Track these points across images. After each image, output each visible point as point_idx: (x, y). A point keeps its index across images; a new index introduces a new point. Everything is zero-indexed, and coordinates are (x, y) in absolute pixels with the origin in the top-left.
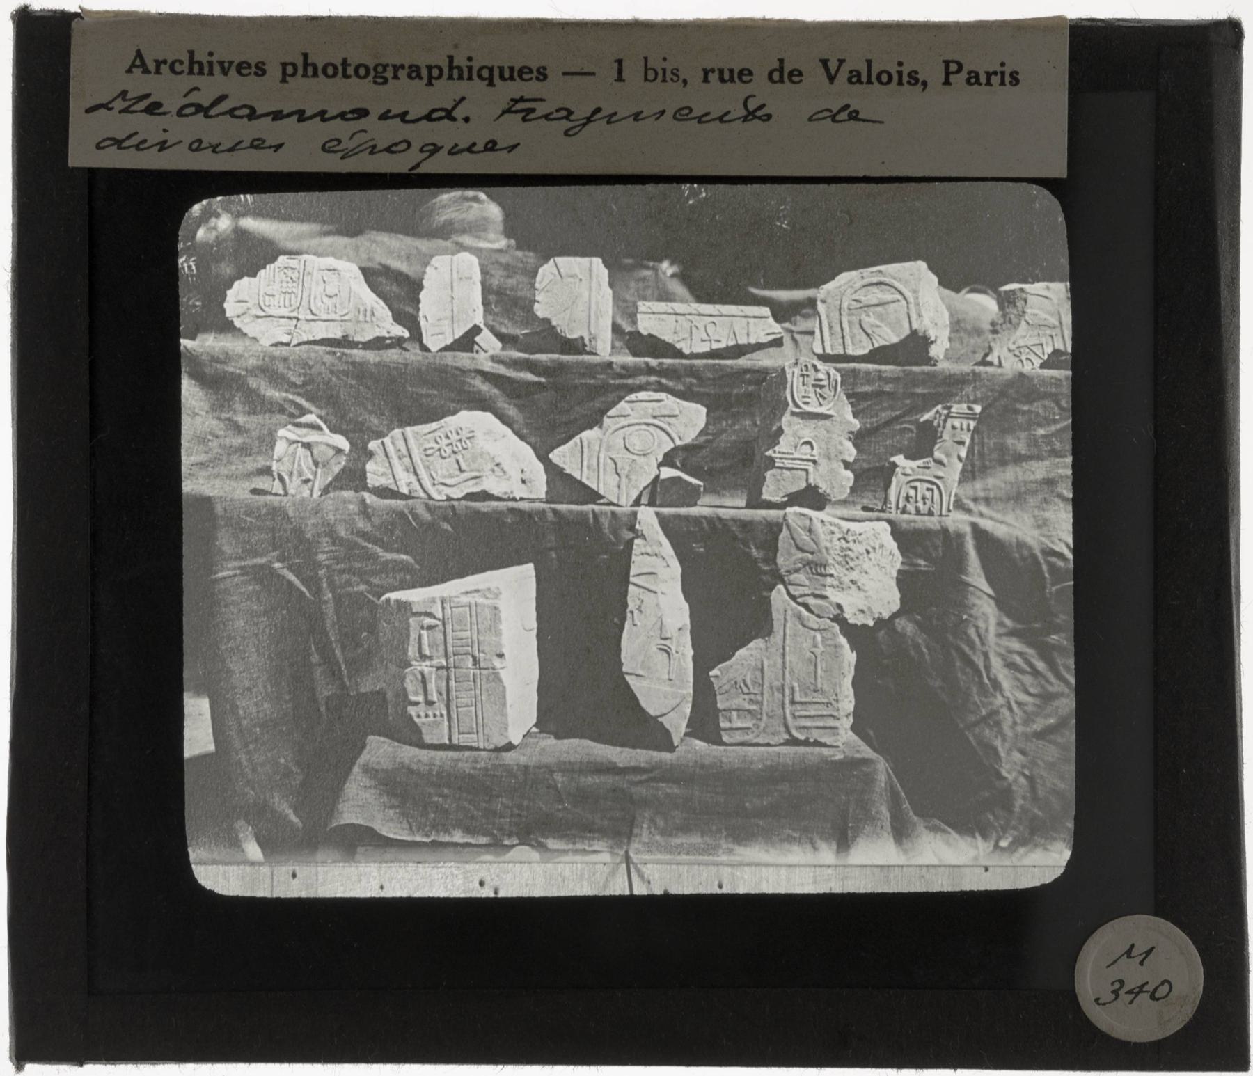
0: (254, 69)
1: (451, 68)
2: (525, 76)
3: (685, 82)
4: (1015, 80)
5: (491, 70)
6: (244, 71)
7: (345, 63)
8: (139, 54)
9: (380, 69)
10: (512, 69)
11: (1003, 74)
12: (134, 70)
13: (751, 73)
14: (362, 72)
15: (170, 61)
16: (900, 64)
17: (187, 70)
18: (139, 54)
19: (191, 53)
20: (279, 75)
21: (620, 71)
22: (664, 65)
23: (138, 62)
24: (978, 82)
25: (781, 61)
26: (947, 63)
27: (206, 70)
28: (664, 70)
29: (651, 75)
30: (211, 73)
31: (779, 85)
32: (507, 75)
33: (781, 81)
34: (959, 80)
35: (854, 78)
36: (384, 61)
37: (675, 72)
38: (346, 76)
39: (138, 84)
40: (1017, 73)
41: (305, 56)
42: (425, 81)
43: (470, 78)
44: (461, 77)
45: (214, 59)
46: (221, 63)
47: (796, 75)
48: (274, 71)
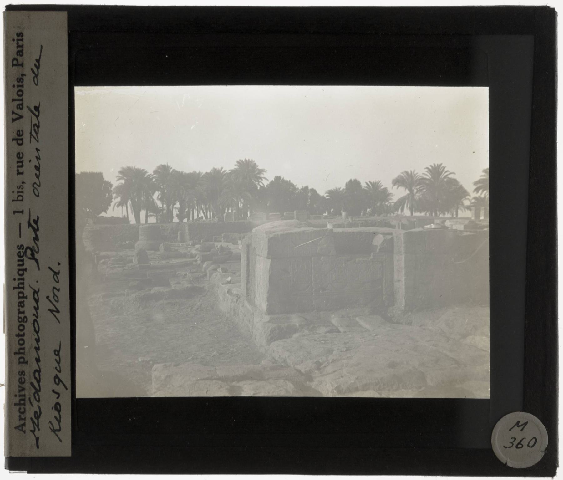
1: (19, 288)
3: (23, 183)
5: (19, 270)
6: (23, 380)
7: (18, 335)
9: (20, 320)
10: (19, 261)
11: (18, 40)
12: (24, 430)
13: (19, 154)
16: (14, 86)
20: (24, 365)
21: (18, 212)
22: (16, 193)
23: (20, 428)
24: (22, 51)
25: (13, 140)
27: (23, 398)
28: (18, 192)
29: (20, 198)
31: (24, 141)
32: (21, 263)
33: (22, 140)
34: (20, 59)
36: (17, 318)
37: (19, 187)
38: (24, 335)
39: (29, 426)
40: (17, 33)
42: (25, 300)
44: (23, 284)
46: (20, 391)
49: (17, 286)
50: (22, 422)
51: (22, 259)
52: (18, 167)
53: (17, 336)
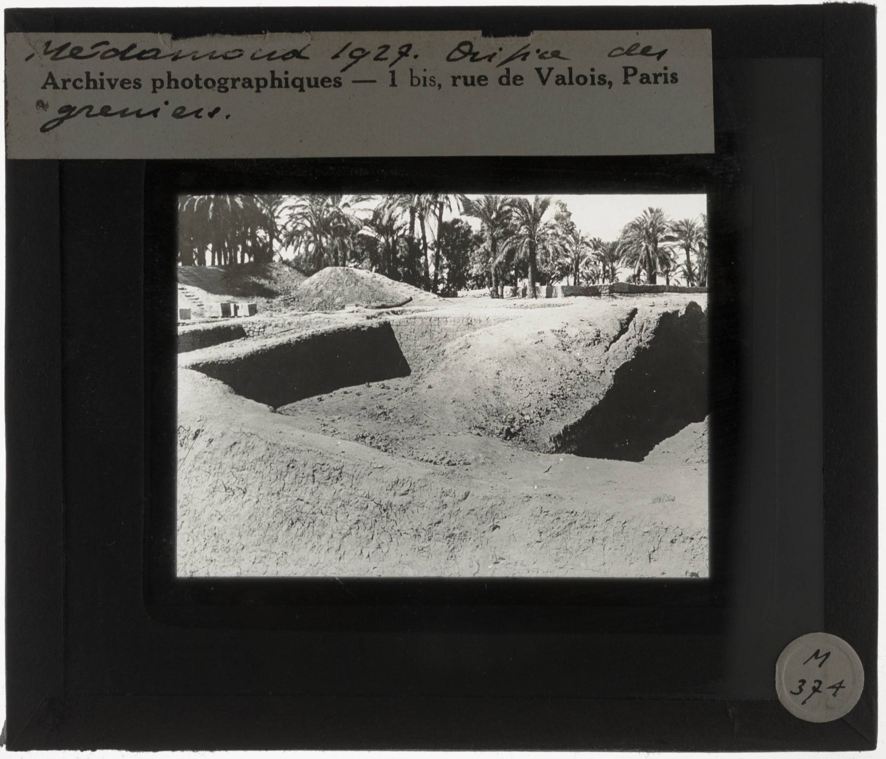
0: (133, 84)
1: (273, 79)
2: (326, 84)
3: (440, 86)
4: (675, 78)
5: (301, 80)
6: (126, 86)
7: (198, 78)
8: (51, 75)
9: (223, 81)
10: (316, 79)
11: (666, 75)
14: (209, 83)
15: (73, 80)
17: (85, 86)
18: (51, 75)
19: (88, 74)
21: (393, 80)
22: (424, 74)
23: (50, 81)
24: (648, 82)
25: (508, 70)
26: (626, 68)
27: (99, 86)
28: (425, 78)
29: (415, 81)
30: (102, 87)
32: (313, 83)
33: (508, 83)
34: (634, 80)
35: (560, 80)
38: (198, 87)
40: (676, 74)
41: (169, 73)
42: (255, 89)
43: (287, 86)
44: (280, 86)
45: (104, 77)
46: (109, 80)
47: (518, 79)
48: (147, 85)
49: (276, 76)
50: (60, 84)
51: (319, 84)
52: (465, 78)
53: (197, 76)
